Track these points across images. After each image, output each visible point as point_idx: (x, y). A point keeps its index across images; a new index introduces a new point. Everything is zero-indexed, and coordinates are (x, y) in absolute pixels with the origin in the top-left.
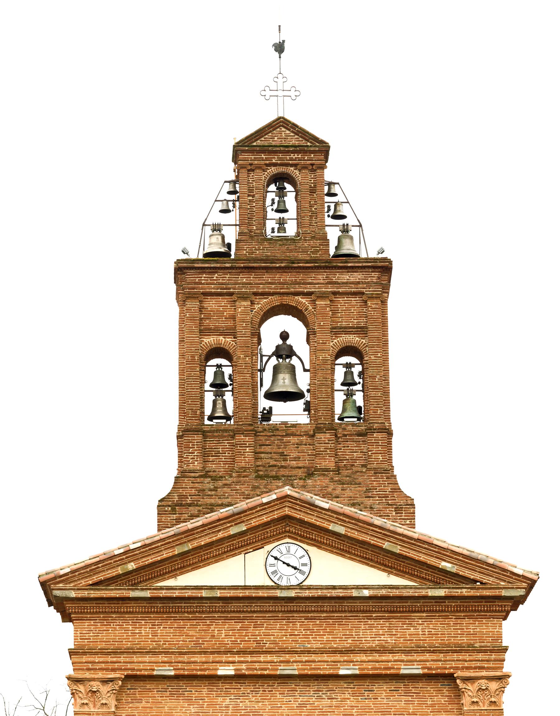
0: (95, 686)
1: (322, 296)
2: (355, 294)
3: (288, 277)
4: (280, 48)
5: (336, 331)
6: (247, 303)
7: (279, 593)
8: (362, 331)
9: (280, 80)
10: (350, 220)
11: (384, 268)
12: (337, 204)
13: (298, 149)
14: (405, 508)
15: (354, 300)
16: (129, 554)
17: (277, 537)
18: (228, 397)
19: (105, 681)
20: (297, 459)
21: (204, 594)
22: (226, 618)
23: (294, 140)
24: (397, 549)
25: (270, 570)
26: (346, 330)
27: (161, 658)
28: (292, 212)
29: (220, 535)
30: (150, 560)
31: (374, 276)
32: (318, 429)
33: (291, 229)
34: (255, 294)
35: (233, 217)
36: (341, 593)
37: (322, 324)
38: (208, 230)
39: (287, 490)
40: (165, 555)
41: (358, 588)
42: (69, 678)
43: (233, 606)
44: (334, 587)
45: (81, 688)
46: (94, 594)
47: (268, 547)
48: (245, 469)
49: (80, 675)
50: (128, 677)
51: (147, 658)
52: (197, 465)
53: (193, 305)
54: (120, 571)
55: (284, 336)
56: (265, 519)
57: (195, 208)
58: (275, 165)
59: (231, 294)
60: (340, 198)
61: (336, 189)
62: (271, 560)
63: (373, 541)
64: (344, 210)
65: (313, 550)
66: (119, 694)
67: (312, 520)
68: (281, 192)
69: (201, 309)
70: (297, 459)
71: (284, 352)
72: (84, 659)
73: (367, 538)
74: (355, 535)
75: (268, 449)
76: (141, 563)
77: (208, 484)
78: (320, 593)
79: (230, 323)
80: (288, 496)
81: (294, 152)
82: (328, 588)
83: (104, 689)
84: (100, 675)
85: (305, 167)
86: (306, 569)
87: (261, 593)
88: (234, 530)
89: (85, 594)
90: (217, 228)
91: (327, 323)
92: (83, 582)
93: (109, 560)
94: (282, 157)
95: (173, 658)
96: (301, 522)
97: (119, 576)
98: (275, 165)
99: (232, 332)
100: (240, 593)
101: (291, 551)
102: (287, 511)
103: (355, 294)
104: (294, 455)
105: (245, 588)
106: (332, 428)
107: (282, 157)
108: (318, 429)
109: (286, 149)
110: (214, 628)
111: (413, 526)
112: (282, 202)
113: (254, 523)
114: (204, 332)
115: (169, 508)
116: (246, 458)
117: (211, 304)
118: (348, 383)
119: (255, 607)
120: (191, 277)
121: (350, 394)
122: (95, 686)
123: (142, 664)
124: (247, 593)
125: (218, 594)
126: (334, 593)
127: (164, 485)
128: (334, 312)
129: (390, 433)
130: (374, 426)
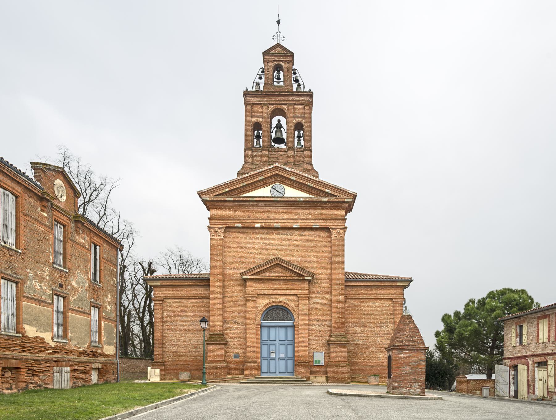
0: (217, 229)
1: (291, 105)
2: (301, 104)
3: (280, 98)
4: (279, 22)
5: (295, 117)
6: (266, 107)
7: (274, 199)
8: (303, 117)
9: (279, 34)
10: (301, 82)
11: (310, 95)
12: (296, 76)
13: (283, 55)
14: (316, 174)
15: (301, 107)
16: (225, 185)
17: (274, 182)
18: (261, 140)
19: (220, 228)
20: (282, 159)
21: (250, 199)
22: (258, 209)
23: (282, 52)
24: (312, 185)
25: (272, 193)
26: (298, 117)
27: (237, 221)
28: (282, 80)
29: (256, 180)
30: (233, 188)
31: (307, 99)
32: (288, 149)
33: (282, 84)
34: (269, 104)
35: (263, 81)
36: (294, 199)
37: (290, 118)
38: (255, 84)
39: (277, 164)
40: (238, 186)
41: (299, 198)
42: (208, 227)
43: (260, 204)
44: (292, 197)
45: (212, 230)
46: (215, 199)
47: (271, 186)
48: (265, 162)
49: (212, 226)
50: (227, 228)
51: (233, 221)
52: (250, 161)
53: (249, 107)
54: (223, 191)
55: (279, 121)
56: (270, 175)
57: (249, 72)
58: (276, 61)
59: (261, 104)
60: (297, 75)
61: (296, 71)
62: (273, 190)
63: (305, 182)
64: (299, 78)
65: (286, 187)
66: (224, 232)
67: (285, 175)
68: (279, 73)
69: (252, 109)
70: (282, 159)
71: (279, 126)
72: (213, 221)
73: (302, 181)
74: (299, 180)
75: (273, 156)
76: (230, 189)
77: (253, 166)
78: (287, 199)
79: (261, 114)
80: (277, 166)
81: (282, 56)
82: (290, 197)
83: (219, 231)
84: (218, 226)
85: (286, 61)
86: (283, 193)
87: (268, 199)
88: (260, 178)
89: (212, 199)
90: (258, 84)
91: (292, 114)
92: (211, 195)
93: (219, 187)
94: (278, 59)
95: (241, 221)
96: (282, 176)
97: (223, 193)
98: (276, 61)
99: (261, 117)
100: (262, 199)
101: (278, 186)
102: (277, 172)
103: (301, 104)
104: (281, 158)
105: (263, 197)
106: (293, 149)
107: (278, 59)
108: (288, 149)
109: (279, 55)
110: (254, 212)
111: (318, 177)
112: (279, 75)
113: (266, 176)
114: (252, 117)
115: (239, 173)
116: (266, 158)
117: (255, 107)
118: (299, 137)
119: (267, 204)
120: (249, 98)
121: (299, 140)
122: (217, 229)
123: (231, 223)
124: (264, 199)
125: (255, 199)
126: (292, 199)
127: (240, 167)
128: (294, 111)
129: (311, 151)
130: (307, 149)
